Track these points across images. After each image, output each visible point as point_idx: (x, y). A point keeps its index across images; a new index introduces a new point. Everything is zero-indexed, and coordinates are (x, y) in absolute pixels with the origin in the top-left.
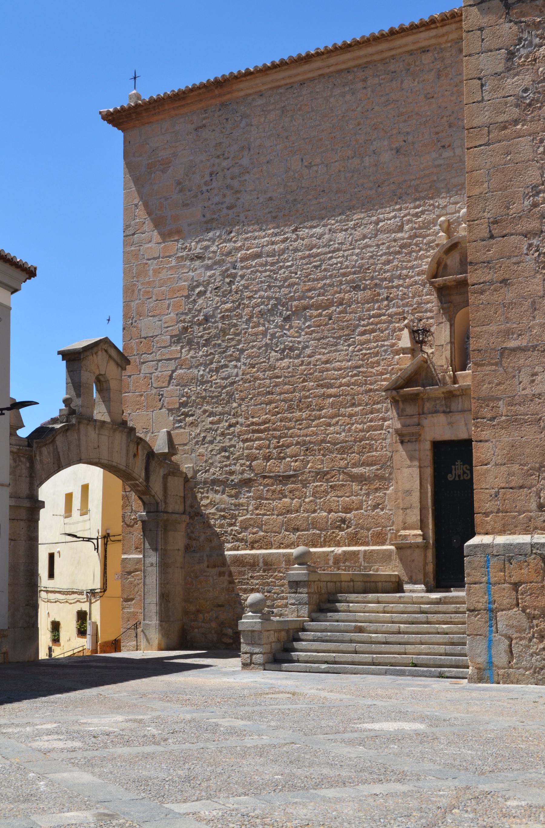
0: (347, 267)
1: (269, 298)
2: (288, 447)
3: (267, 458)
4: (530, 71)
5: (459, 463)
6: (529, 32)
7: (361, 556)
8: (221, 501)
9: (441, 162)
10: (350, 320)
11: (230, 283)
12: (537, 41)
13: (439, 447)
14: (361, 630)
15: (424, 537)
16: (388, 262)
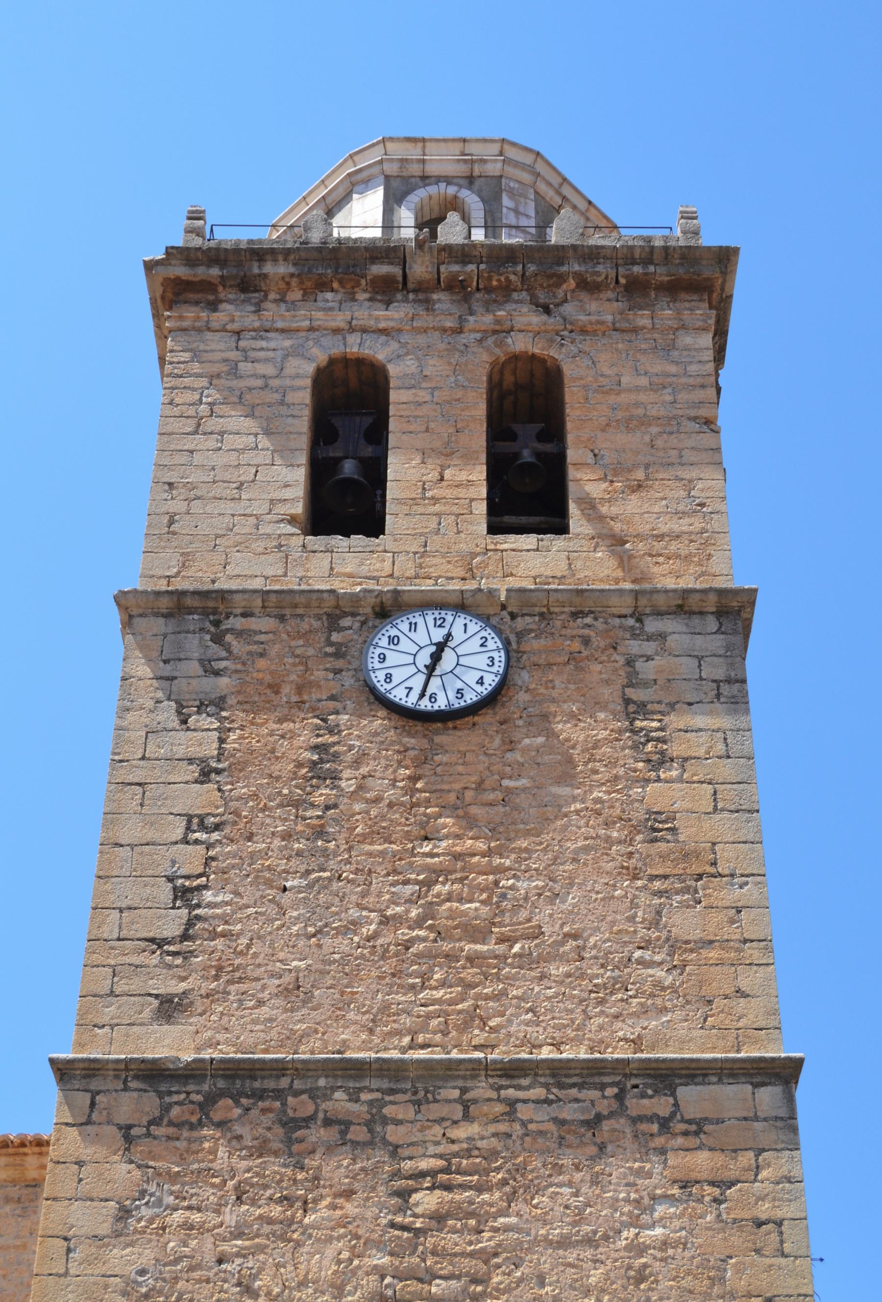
4: (154, 1243)
6: (158, 1185)
12: (170, 1200)
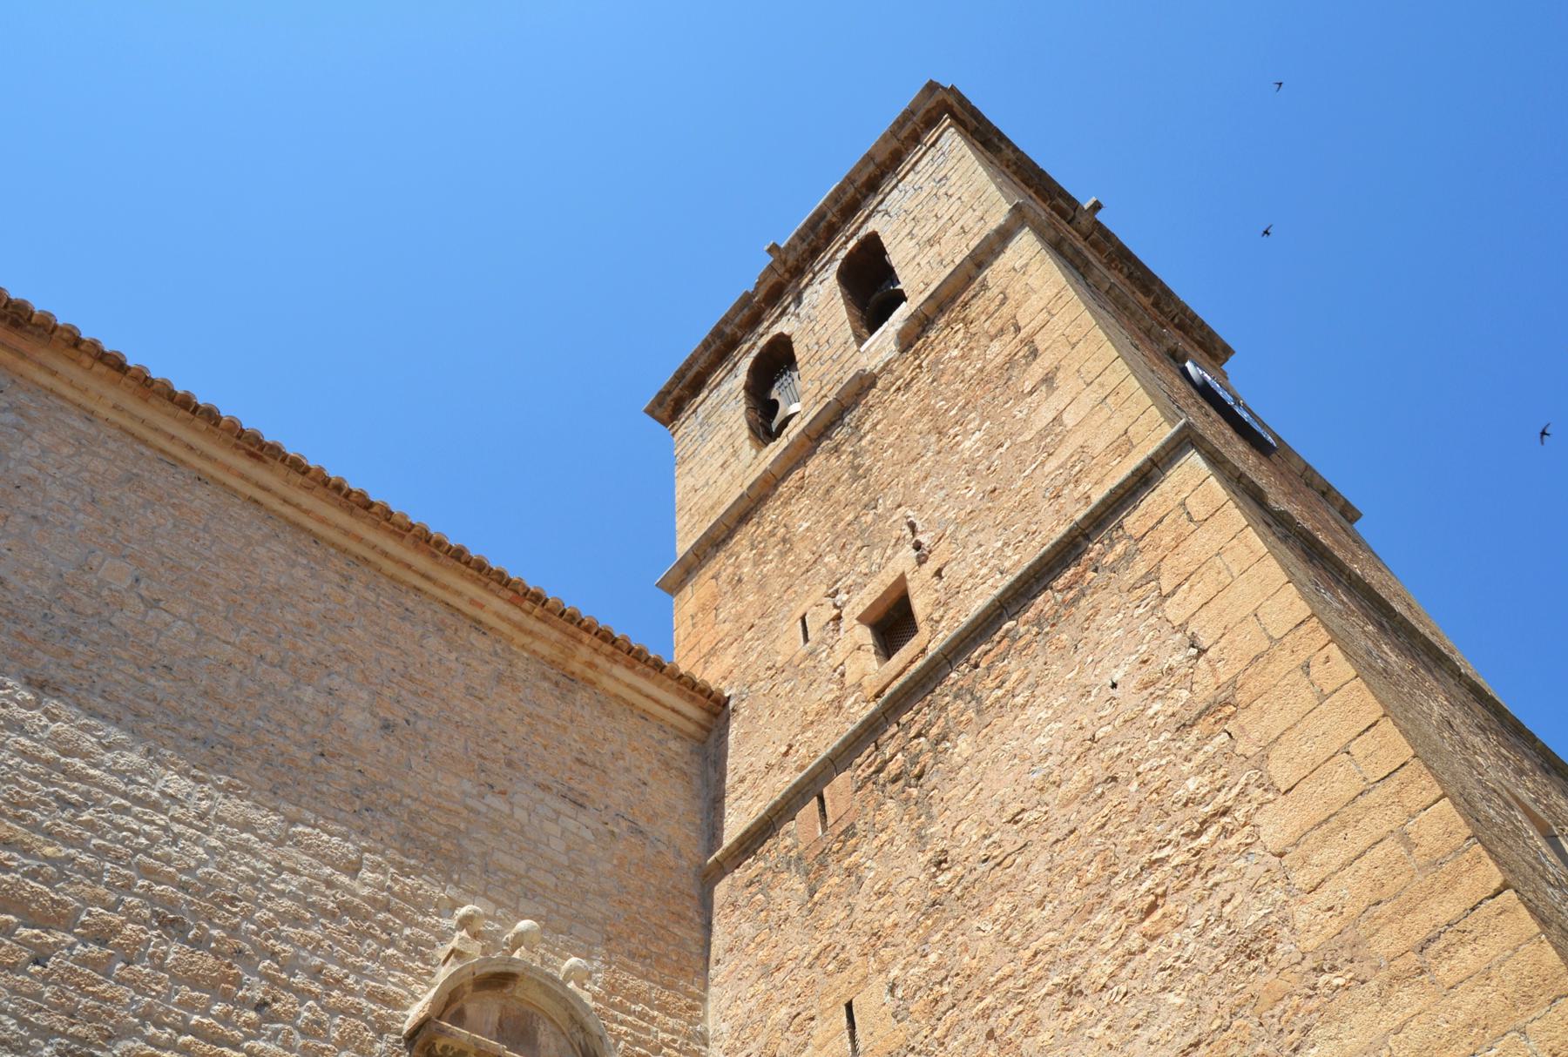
0: (168, 860)
9: (483, 809)
10: (112, 999)
16: (297, 921)
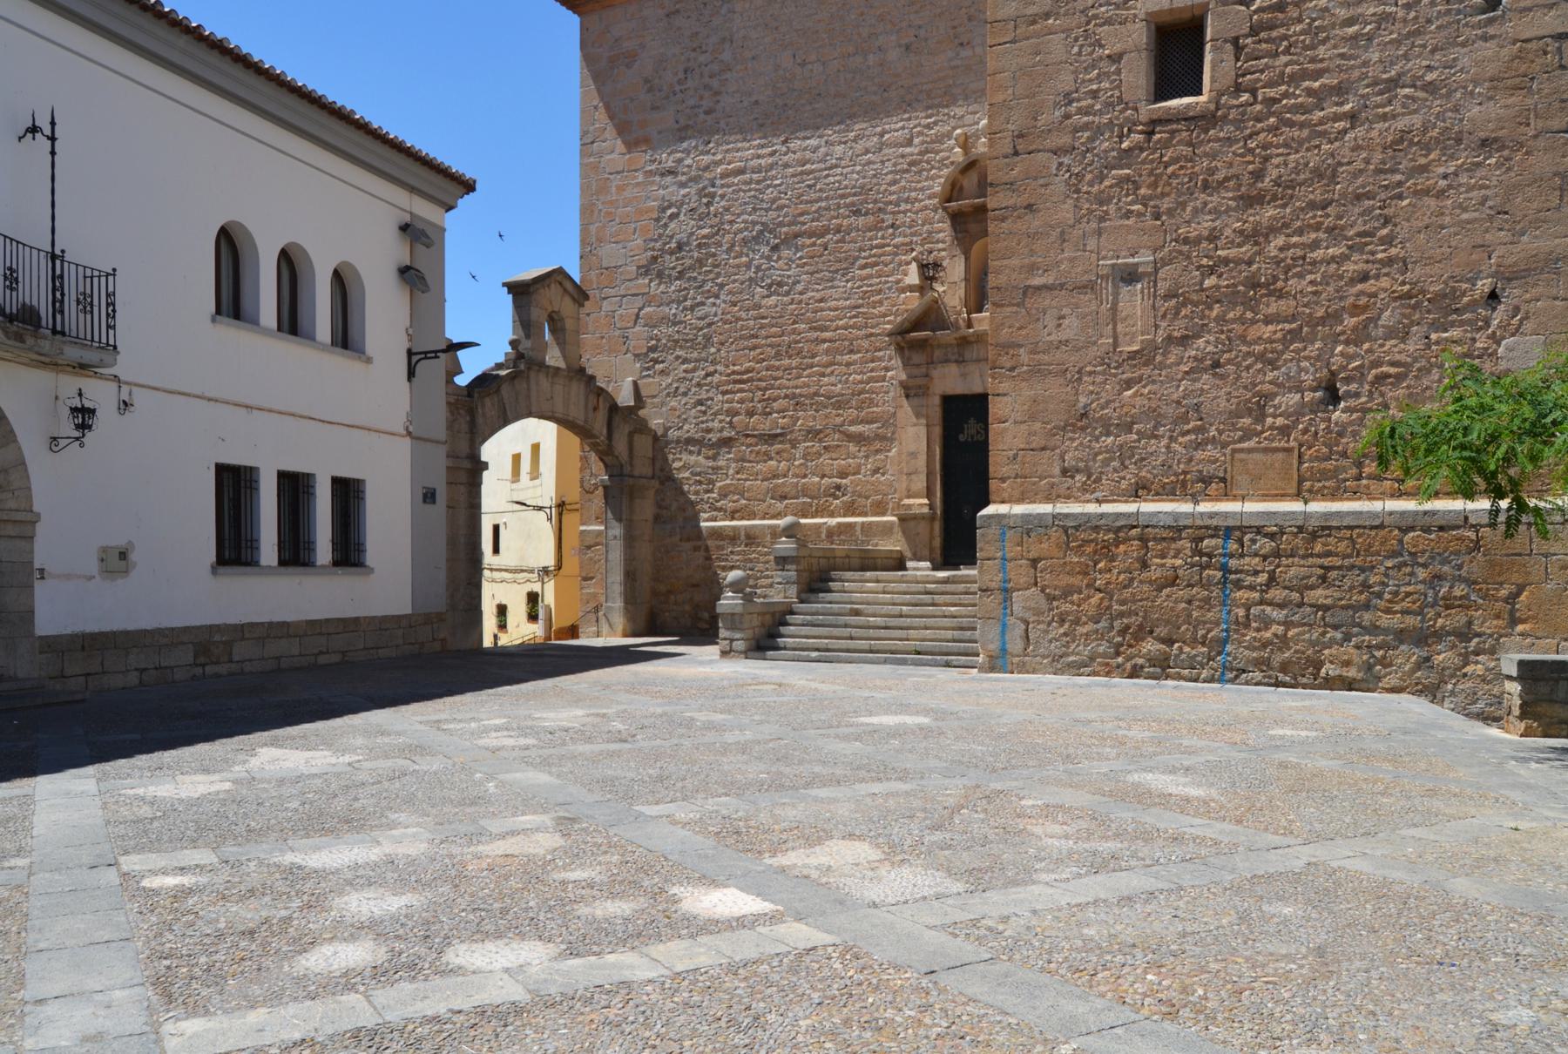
1: (754, 223)
2: (775, 400)
3: (751, 414)
5: (972, 421)
7: (858, 528)
8: (697, 464)
9: (959, 62)
11: (708, 204)
13: (949, 401)
14: (857, 613)
15: (931, 506)
16: (894, 182)
